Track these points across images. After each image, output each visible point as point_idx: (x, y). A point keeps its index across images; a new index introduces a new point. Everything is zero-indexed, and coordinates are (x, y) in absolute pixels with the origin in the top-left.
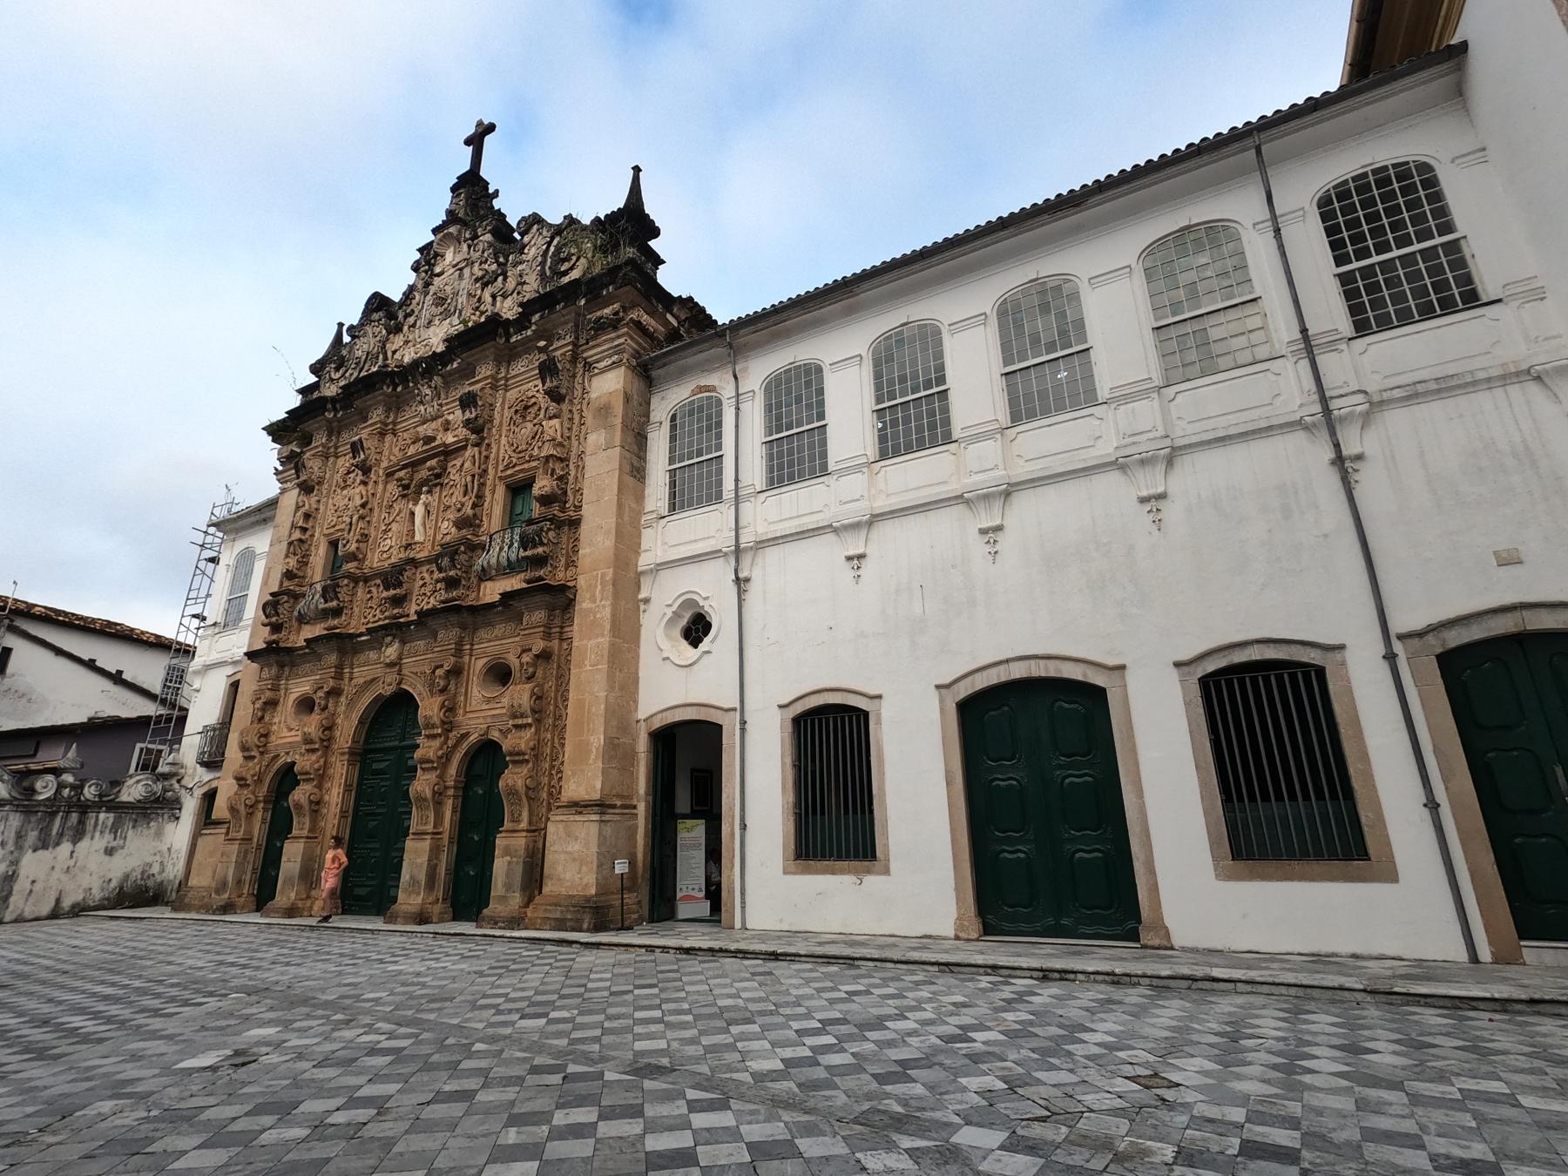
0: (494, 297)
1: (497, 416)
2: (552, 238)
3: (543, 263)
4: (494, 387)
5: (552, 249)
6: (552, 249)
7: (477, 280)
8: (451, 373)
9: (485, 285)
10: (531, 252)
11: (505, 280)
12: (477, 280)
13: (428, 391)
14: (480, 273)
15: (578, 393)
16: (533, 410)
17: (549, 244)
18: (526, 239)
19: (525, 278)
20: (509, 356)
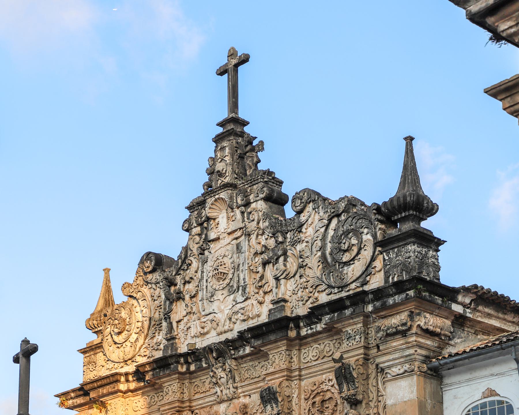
0: (277, 279)
1: (294, 407)
2: (330, 221)
3: (322, 248)
4: (289, 378)
5: (331, 233)
6: (331, 233)
7: (256, 254)
8: (242, 357)
9: (265, 264)
10: (309, 232)
11: (285, 260)
12: (256, 254)
13: (223, 374)
14: (259, 248)
15: (373, 395)
16: (330, 405)
17: (327, 226)
18: (303, 218)
19: (307, 261)
20: (302, 341)
